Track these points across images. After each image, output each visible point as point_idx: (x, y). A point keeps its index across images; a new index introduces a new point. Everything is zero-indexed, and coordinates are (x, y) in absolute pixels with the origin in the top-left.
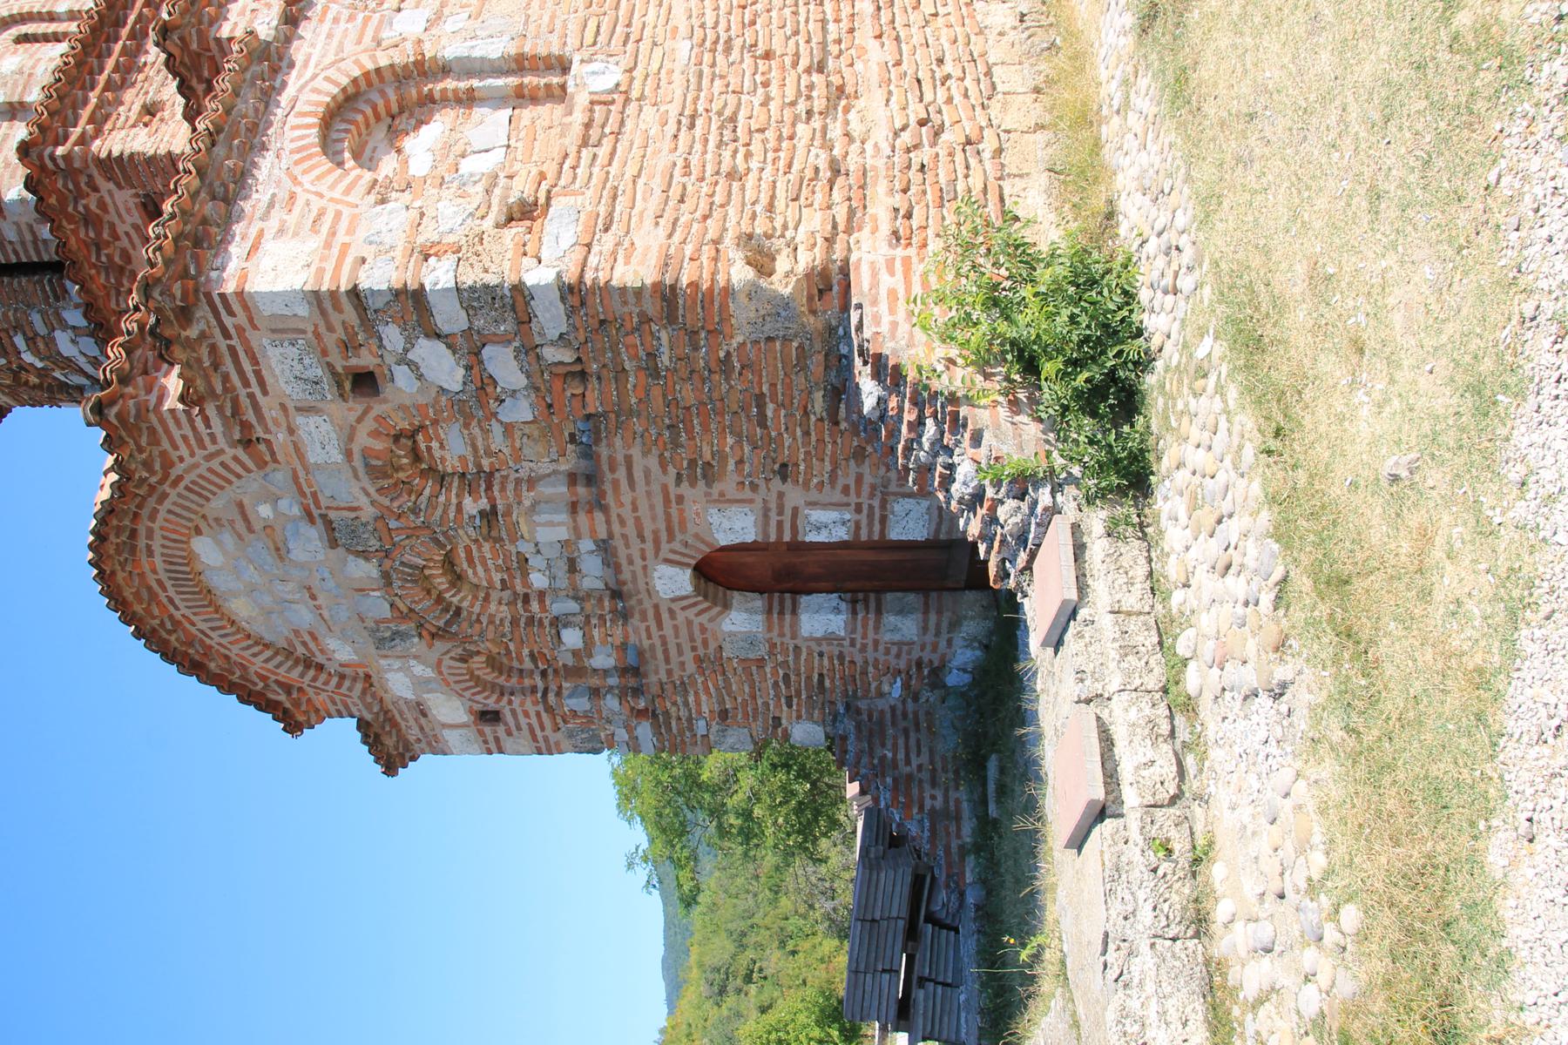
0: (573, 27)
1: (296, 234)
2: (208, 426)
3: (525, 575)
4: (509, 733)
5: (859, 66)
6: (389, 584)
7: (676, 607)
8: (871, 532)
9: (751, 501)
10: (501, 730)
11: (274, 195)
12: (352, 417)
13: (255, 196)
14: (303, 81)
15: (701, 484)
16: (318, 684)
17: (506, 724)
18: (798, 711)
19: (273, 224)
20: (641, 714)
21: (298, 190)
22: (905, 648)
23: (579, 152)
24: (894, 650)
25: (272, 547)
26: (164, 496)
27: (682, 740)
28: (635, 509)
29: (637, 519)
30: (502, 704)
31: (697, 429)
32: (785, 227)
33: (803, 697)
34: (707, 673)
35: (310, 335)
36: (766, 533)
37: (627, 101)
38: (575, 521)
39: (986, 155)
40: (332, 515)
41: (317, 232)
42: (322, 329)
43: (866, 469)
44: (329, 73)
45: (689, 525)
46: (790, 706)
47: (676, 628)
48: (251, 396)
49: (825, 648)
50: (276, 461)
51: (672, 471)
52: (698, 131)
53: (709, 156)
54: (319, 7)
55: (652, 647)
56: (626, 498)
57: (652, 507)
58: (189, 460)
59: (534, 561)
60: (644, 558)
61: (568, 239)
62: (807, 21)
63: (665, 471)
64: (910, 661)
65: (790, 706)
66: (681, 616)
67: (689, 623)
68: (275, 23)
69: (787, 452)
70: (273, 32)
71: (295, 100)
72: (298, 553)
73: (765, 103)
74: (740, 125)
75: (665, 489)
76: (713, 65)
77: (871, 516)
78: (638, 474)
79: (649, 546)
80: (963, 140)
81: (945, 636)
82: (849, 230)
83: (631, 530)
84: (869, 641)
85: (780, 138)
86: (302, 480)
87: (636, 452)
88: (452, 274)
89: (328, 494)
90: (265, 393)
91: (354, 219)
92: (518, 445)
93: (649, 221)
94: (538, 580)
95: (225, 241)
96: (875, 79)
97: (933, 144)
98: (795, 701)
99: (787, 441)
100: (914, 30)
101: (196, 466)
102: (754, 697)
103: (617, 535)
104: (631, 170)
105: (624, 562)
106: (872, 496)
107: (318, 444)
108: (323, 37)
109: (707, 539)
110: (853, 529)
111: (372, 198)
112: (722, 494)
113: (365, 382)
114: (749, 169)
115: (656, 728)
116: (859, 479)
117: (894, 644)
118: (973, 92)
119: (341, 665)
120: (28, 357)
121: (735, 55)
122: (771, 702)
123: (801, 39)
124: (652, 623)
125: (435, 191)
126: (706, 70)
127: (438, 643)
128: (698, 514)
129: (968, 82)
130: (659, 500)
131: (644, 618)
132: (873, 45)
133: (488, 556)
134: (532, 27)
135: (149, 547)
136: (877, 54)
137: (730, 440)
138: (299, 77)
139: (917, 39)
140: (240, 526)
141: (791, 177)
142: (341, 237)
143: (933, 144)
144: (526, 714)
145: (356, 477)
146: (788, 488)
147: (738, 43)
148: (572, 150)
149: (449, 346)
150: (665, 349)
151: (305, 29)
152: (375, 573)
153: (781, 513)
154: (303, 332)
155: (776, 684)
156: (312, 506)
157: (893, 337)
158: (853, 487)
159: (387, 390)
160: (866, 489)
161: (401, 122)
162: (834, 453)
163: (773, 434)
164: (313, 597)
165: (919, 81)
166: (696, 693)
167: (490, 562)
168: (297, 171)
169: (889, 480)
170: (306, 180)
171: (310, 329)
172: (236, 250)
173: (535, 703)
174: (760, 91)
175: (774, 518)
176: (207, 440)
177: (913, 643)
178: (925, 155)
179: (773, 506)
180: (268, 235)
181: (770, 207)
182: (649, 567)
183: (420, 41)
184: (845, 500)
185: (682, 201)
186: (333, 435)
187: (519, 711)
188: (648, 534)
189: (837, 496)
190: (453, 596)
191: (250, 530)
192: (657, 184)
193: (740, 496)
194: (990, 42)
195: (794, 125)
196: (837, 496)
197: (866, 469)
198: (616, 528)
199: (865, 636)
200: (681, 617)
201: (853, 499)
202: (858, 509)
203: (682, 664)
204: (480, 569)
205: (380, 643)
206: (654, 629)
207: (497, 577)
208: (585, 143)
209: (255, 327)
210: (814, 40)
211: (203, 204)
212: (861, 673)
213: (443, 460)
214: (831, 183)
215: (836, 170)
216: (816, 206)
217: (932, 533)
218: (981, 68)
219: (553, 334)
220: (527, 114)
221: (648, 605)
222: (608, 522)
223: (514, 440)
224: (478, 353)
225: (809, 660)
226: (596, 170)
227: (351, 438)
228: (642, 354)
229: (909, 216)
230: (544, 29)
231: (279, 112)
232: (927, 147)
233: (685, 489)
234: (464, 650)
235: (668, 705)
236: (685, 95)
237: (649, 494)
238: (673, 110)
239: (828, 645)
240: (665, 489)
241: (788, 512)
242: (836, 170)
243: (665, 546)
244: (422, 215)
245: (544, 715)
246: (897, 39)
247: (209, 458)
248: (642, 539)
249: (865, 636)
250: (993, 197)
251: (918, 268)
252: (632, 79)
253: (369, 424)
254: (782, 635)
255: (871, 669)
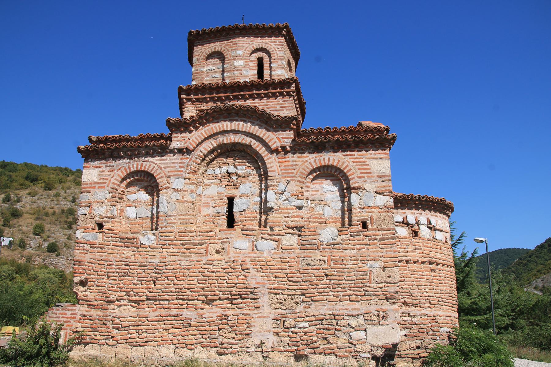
0: (170, 229)
1: (99, 175)
5: (148, 309)
11: (114, 166)
13: (114, 162)
14: (154, 161)
19: (104, 169)
21: (115, 171)
23: (118, 238)
32: (90, 289)
37: (138, 248)
39: (107, 341)
41: (100, 180)
44: (156, 167)
52: (123, 266)
53: (114, 270)
54: (188, 156)
61: (87, 238)
62: (168, 295)
68: (176, 147)
70: (172, 148)
71: (147, 161)
73: (134, 284)
74: (127, 277)
76: (148, 269)
80: (113, 335)
82: (88, 305)
85: (120, 288)
88: (81, 214)
91: (104, 187)
93: (92, 257)
95: (99, 159)
96: (141, 314)
97: (113, 328)
100: (163, 326)
104: (109, 251)
108: (173, 161)
111: (111, 190)
114: (109, 280)
118: (132, 340)
121: (153, 275)
123: (161, 293)
125: (110, 204)
126: (147, 267)
129: (138, 339)
132: (157, 313)
134: (171, 218)
136: (153, 315)
138: (157, 160)
139: (158, 326)
141: (107, 291)
142: (97, 186)
143: (113, 328)
147: (159, 275)
148: (118, 236)
151: (177, 156)
157: (53, 313)
161: (149, 189)
165: (139, 326)
168: (123, 169)
170: (119, 172)
172: (97, 163)
174: (138, 282)
178: (110, 324)
180: (100, 169)
181: (97, 286)
183: (168, 188)
185: (99, 264)
192: (104, 258)
194: (154, 348)
195: (125, 291)
208: (121, 239)
210: (160, 297)
211: (108, 152)
214: (104, 301)
215: (111, 302)
216: (96, 297)
218: (141, 344)
220: (149, 220)
226: (111, 242)
229: (90, 320)
230: (169, 221)
231: (143, 158)
232: (112, 326)
236: (137, 262)
238: (132, 259)
242: (111, 302)
244: (102, 203)
246: (159, 321)
250: (93, 341)
251: (72, 321)
252: (146, 248)
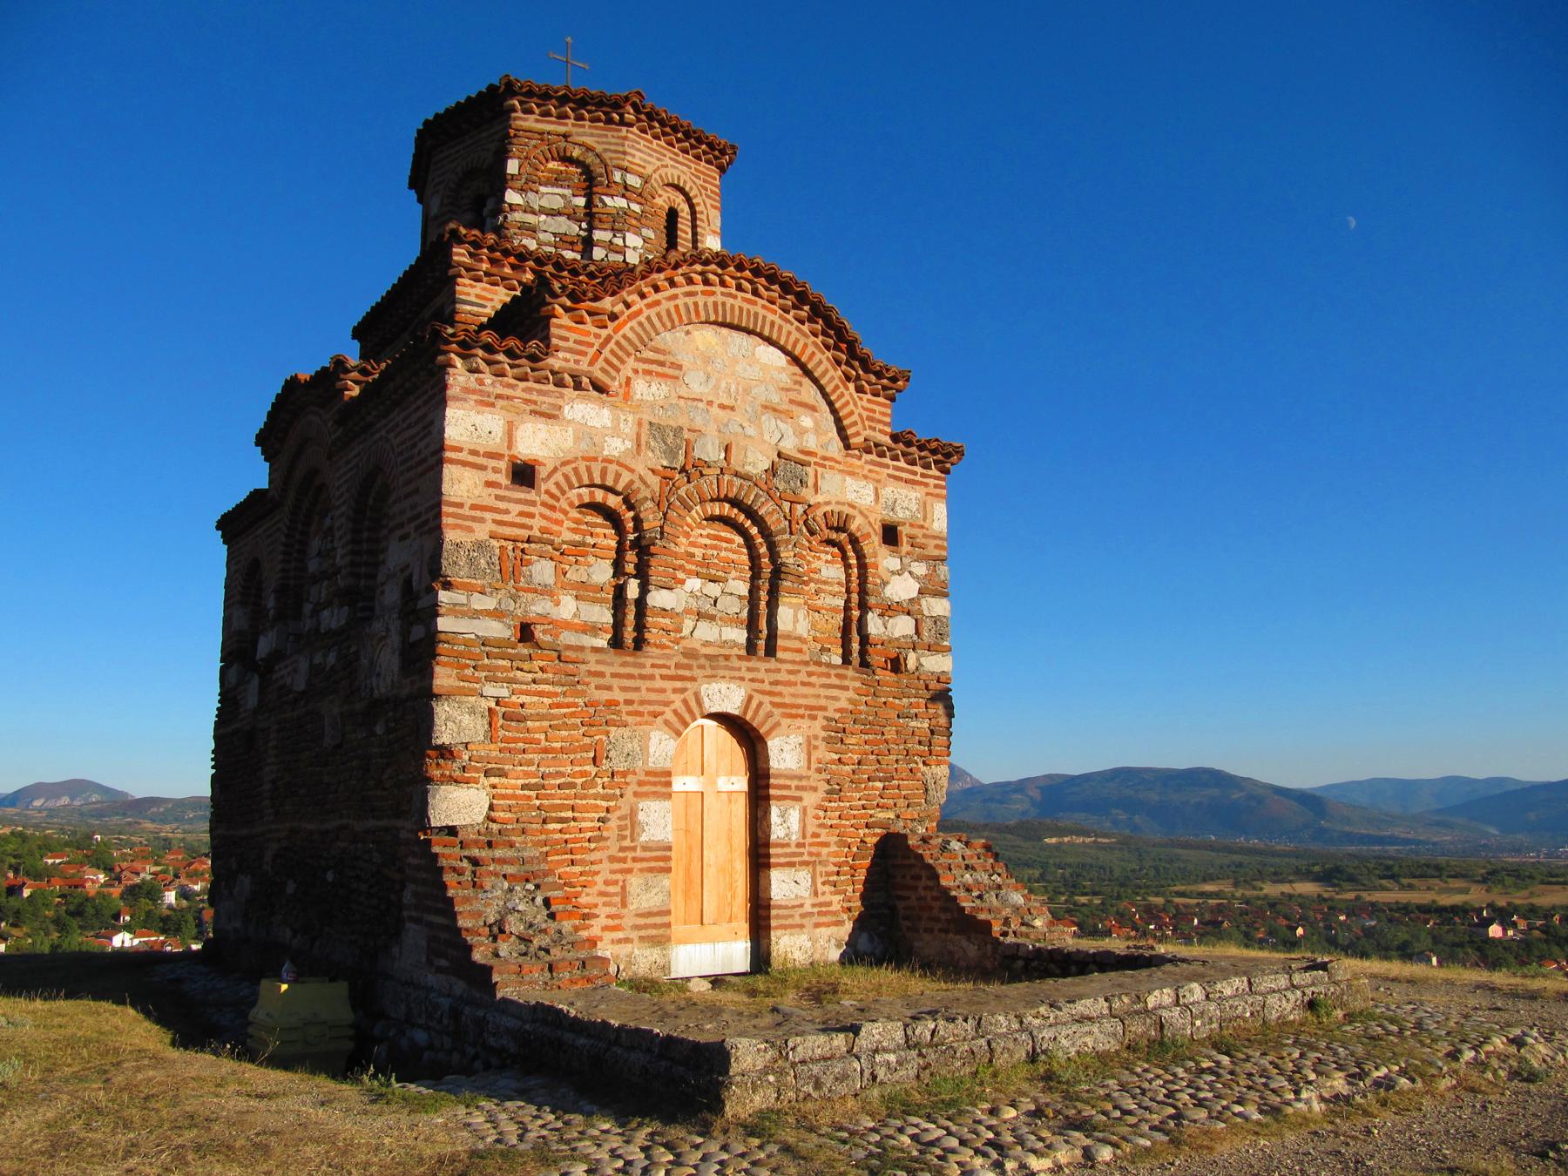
2: (880, 431)
3: (698, 575)
4: (489, 484)
6: (737, 474)
7: (689, 695)
8: (778, 855)
9: (809, 768)
10: (504, 479)
12: (873, 521)
15: (823, 734)
16: (612, 345)
17: (507, 488)
18: (514, 797)
20: (526, 632)
22: (617, 899)
24: (611, 889)
25: (777, 407)
26: (835, 370)
27: (467, 666)
28: (803, 684)
29: (795, 684)
30: (545, 498)
31: (866, 737)
33: (538, 802)
34: (592, 710)
35: (922, 523)
36: (778, 776)
38: (796, 638)
40: (811, 471)
42: (925, 531)
43: (834, 848)
45: (789, 721)
46: (523, 787)
47: (663, 691)
48: (887, 466)
49: (613, 823)
50: (848, 455)
51: (837, 716)
55: (642, 666)
56: (813, 679)
57: (805, 696)
58: (859, 403)
59: (714, 589)
60: (752, 680)
63: (836, 710)
64: (596, 906)
65: (523, 787)
66: (677, 698)
67: (667, 704)
69: (848, 794)
72: (769, 422)
75: (824, 709)
77: (794, 854)
78: (835, 692)
79: (767, 687)
81: (634, 935)
83: (783, 677)
84: (629, 865)
86: (832, 464)
87: (851, 694)
89: (826, 476)
90: (890, 476)
92: (823, 611)
94: (694, 584)
98: (534, 794)
99: (858, 795)
101: (855, 404)
102: (545, 751)
103: (779, 665)
105: (750, 664)
106: (811, 854)
107: (857, 489)
109: (774, 733)
110: (781, 841)
112: (816, 747)
113: (890, 535)
115: (500, 643)
116: (826, 845)
117: (624, 888)
119: (628, 380)
120: (621, 203)
122: (533, 768)
124: (672, 672)
127: (658, 479)
128: (799, 728)
130: (812, 702)
131: (678, 666)
133: (723, 554)
135: (792, 324)
137: (856, 757)
140: (793, 395)
144: (532, 516)
145: (838, 503)
146: (821, 794)
149: (911, 600)
150: (919, 725)
152: (749, 469)
153: (797, 788)
154: (925, 519)
155: (559, 774)
156: (815, 460)
158: (818, 840)
159: (884, 550)
160: (814, 849)
162: (844, 826)
163: (863, 786)
164: (722, 406)
166: (556, 695)
167: (715, 552)
169: (826, 866)
171: (926, 525)
173: (543, 530)
175: (794, 783)
176: (873, 424)
177: (624, 904)
179: (804, 783)
182: (743, 683)
184: (808, 835)
186: (864, 502)
187: (531, 509)
188: (779, 688)
189: (810, 830)
190: (697, 512)
191: (792, 402)
193: (813, 759)
196: (810, 830)
197: (834, 848)
198: (785, 667)
199: (635, 860)
200: (673, 697)
201: (809, 840)
202: (799, 845)
203: (609, 688)
204: (708, 542)
205: (657, 429)
206: (664, 672)
207: (698, 552)
209: (927, 494)
212: (572, 861)
213: (819, 558)
217: (779, 903)
219: (923, 660)
221: (697, 672)
222: (793, 662)
223: (826, 610)
224: (908, 614)
225: (596, 808)
227: (861, 513)
228: (913, 711)
233: (820, 722)
234: (646, 499)
235: (542, 664)
237: (819, 696)
239: (621, 828)
240: (824, 709)
241: (798, 794)
243: (767, 699)
245: (525, 533)
247: (860, 415)
248: (776, 683)
249: (635, 860)
253: (868, 529)
254: (640, 783)
255: (577, 869)
